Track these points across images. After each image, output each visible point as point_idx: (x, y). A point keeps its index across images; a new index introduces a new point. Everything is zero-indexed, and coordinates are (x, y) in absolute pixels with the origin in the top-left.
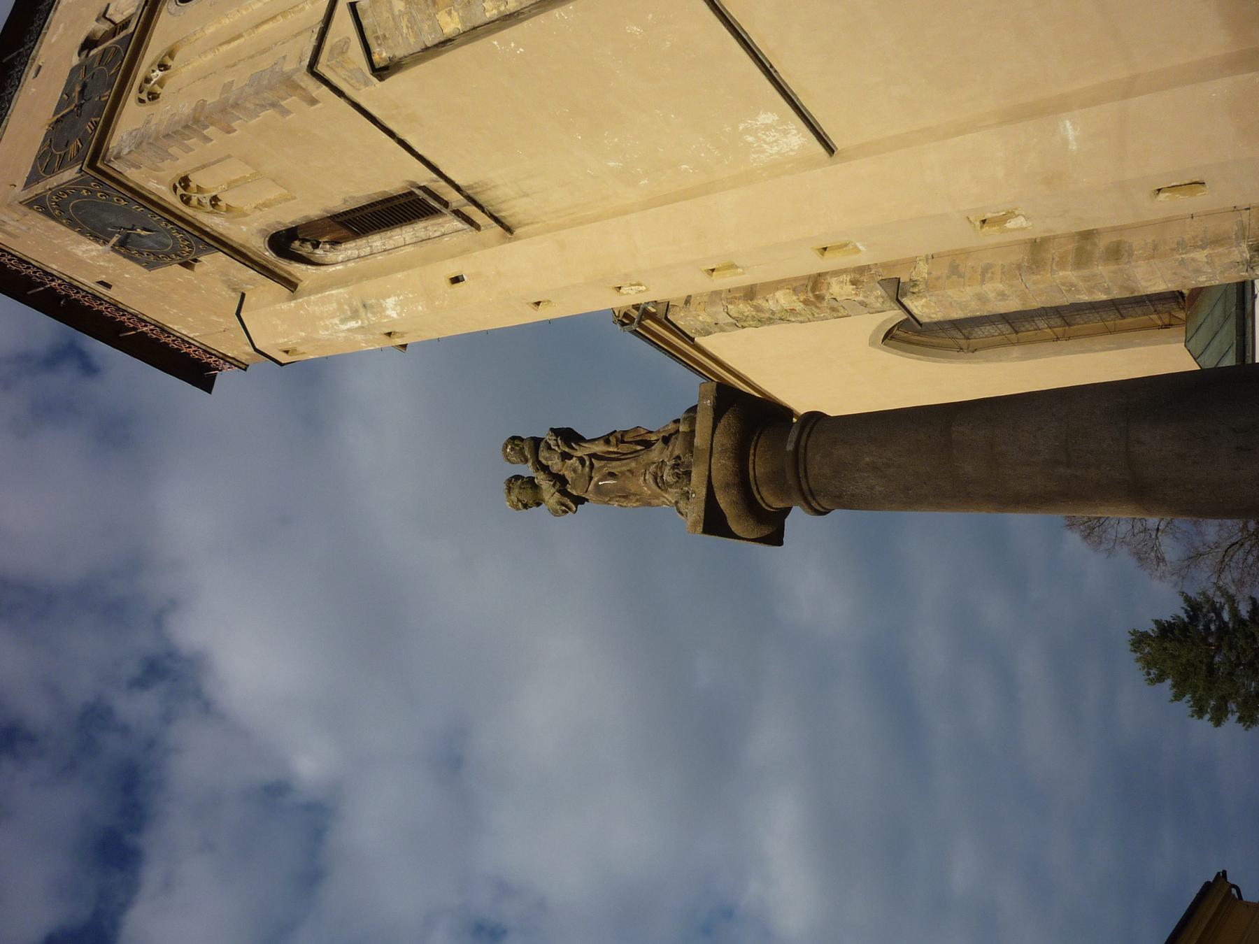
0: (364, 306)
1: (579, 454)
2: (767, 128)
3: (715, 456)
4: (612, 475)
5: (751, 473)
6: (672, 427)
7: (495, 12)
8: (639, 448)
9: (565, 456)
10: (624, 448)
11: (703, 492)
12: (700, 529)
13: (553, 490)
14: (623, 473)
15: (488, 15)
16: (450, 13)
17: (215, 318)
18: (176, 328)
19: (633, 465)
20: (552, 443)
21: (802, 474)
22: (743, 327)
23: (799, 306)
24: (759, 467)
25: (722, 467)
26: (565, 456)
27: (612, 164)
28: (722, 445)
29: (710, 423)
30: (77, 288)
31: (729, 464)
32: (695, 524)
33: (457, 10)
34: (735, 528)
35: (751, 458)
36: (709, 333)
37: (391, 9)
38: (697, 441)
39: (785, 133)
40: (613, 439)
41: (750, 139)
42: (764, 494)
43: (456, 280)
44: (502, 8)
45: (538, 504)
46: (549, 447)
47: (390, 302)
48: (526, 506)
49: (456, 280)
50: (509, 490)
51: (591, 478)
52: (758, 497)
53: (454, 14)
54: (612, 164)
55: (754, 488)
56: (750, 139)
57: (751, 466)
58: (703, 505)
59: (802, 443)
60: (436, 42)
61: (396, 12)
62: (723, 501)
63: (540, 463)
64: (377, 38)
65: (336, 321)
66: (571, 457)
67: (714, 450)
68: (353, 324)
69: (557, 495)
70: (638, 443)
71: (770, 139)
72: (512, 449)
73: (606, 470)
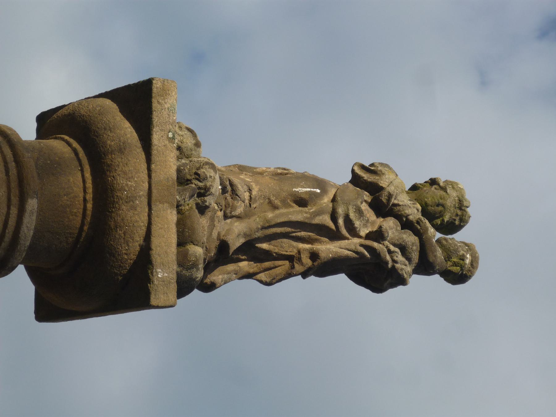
1: (356, 240)
3: (143, 192)
4: (301, 202)
5: (88, 175)
6: (216, 276)
8: (265, 246)
9: (378, 235)
10: (288, 247)
12: (157, 86)
13: (391, 189)
14: (285, 205)
19: (270, 215)
20: (400, 257)
21: (12, 165)
24: (77, 184)
25: (131, 174)
26: (378, 235)
28: (134, 208)
29: (155, 242)
31: (121, 181)
32: (165, 92)
34: (108, 102)
35: (90, 196)
38: (172, 216)
42: (66, 150)
45: (415, 188)
46: (403, 249)
48: (433, 182)
50: (461, 205)
51: (334, 200)
52: (75, 144)
55: (82, 154)
57: (89, 184)
58: (156, 119)
59: (14, 211)
62: (127, 131)
66: (369, 236)
67: (145, 200)
69: (383, 183)
70: (267, 256)
72: (463, 258)
73: (312, 209)
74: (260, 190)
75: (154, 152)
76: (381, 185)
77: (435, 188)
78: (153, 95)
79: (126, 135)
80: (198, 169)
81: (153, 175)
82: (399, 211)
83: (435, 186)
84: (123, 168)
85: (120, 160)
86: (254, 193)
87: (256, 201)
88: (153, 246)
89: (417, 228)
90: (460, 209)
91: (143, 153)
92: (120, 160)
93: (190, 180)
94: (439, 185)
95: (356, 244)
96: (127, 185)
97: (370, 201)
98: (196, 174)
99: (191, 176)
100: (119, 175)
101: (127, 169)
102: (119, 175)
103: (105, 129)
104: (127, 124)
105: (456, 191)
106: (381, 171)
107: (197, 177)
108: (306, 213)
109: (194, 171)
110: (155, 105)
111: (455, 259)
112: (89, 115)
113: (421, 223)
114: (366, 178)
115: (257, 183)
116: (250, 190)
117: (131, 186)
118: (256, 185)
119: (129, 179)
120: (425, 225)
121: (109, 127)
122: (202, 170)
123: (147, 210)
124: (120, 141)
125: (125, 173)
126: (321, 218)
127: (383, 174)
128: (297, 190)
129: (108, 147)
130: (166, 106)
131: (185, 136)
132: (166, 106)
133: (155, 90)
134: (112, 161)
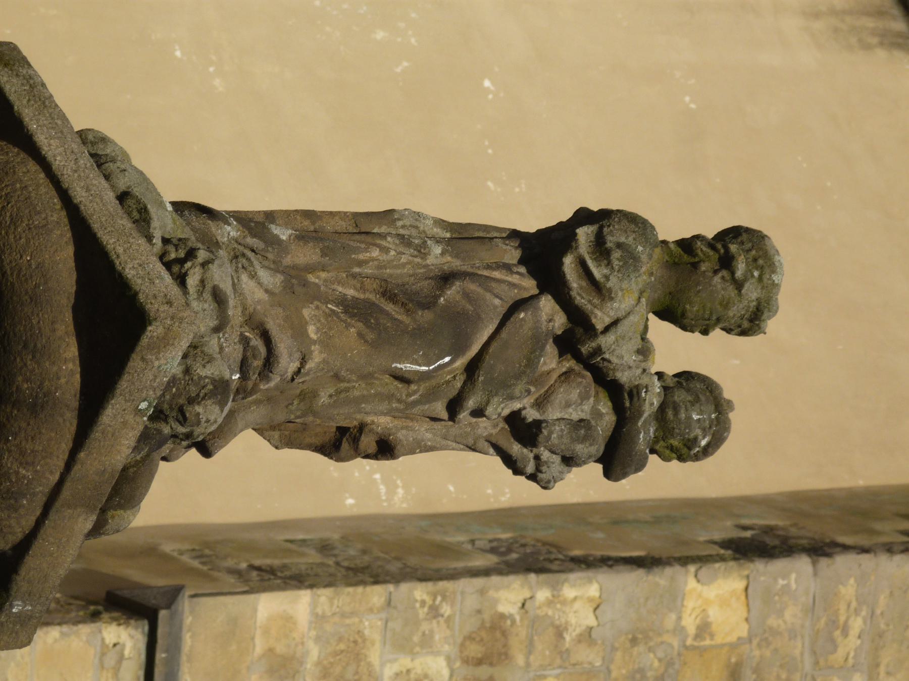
3: (42, 490)
7: (569, 592)
11: (110, 415)
12: (154, 331)
13: (606, 341)
15: (593, 591)
16: (704, 629)
33: (679, 630)
40: (368, 442)
44: (543, 595)
51: (472, 369)
53: (690, 623)
58: (124, 384)
60: (779, 565)
63: (618, 409)
67: (41, 500)
69: (600, 319)
74: (324, 361)
75: (96, 434)
76: (594, 321)
77: (723, 278)
78: (138, 349)
79: (59, 378)
80: (191, 401)
81: (77, 468)
82: (606, 367)
83: (724, 273)
84: (24, 443)
85: (24, 425)
86: (310, 365)
87: (308, 374)
88: (23, 571)
89: (624, 404)
90: (751, 320)
91: (75, 422)
92: (24, 425)
93: (167, 416)
94: (733, 273)
95: (480, 437)
96: (17, 473)
97: (559, 332)
98: (181, 410)
99: (171, 409)
100: (10, 451)
101: (29, 446)
102: (10, 451)
103: (25, 346)
104: (71, 350)
105: (763, 288)
106: (610, 290)
107: (181, 419)
108: (399, 401)
109: (182, 401)
110: (135, 362)
111: (675, 442)
112: (12, 284)
113: (635, 399)
114: (573, 293)
115: (326, 343)
116: (303, 361)
117: (24, 477)
118: (321, 352)
119: (26, 464)
120: (640, 406)
121: (35, 346)
122: (199, 409)
123: (38, 513)
124: (41, 386)
125: (23, 453)
126: (427, 407)
127: (611, 299)
128: (398, 366)
129: (14, 389)
130: (156, 364)
131: (201, 315)
132: (156, 364)
133: (144, 340)
134: (8, 419)
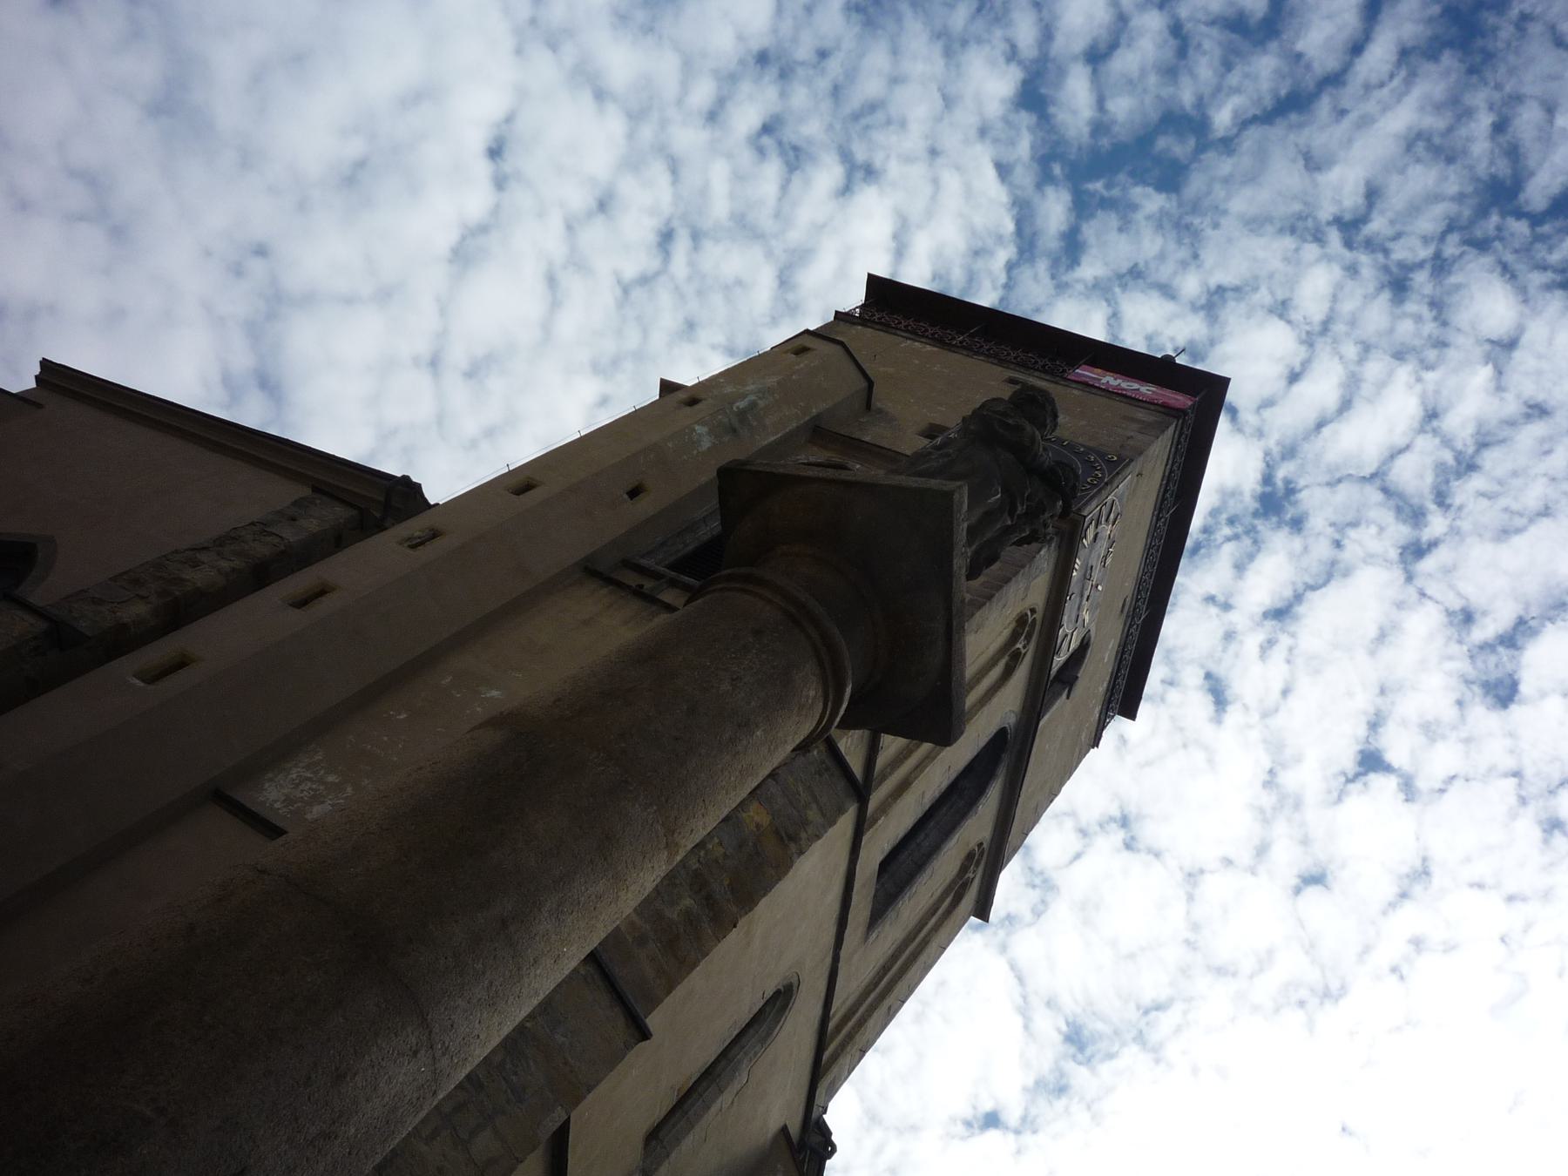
0: (734, 431)
2: (316, 799)
16: (758, 826)
17: (891, 370)
18: (929, 348)
22: (253, 524)
23: (188, 574)
27: (495, 693)
30: (1045, 372)
36: (295, 503)
37: (820, 809)
39: (289, 801)
41: (331, 778)
43: (634, 493)
47: (706, 443)
49: (634, 493)
54: (495, 693)
56: (331, 778)
61: (814, 806)
64: (827, 769)
65: (761, 403)
68: (742, 404)
71: (306, 786)
